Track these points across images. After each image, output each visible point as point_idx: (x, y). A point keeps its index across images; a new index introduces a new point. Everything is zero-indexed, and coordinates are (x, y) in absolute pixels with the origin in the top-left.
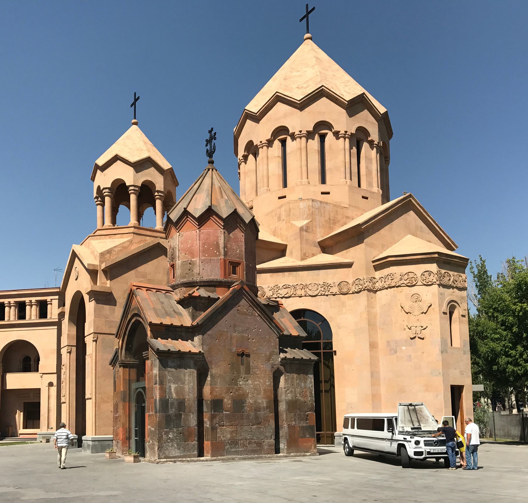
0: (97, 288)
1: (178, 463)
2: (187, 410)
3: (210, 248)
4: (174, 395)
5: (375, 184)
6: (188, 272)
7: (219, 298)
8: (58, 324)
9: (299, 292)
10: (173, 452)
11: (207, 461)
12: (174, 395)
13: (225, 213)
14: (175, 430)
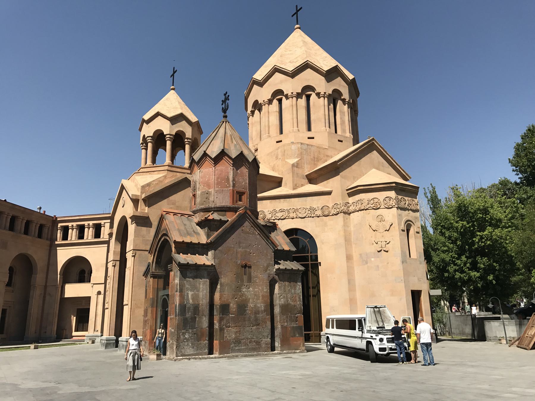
0: (137, 214)
1: (192, 360)
2: (201, 314)
3: (221, 182)
4: (191, 301)
6: (205, 199)
7: (228, 220)
8: (108, 243)
9: (292, 215)
11: (215, 358)
12: (191, 301)
13: (234, 154)
14: (190, 331)
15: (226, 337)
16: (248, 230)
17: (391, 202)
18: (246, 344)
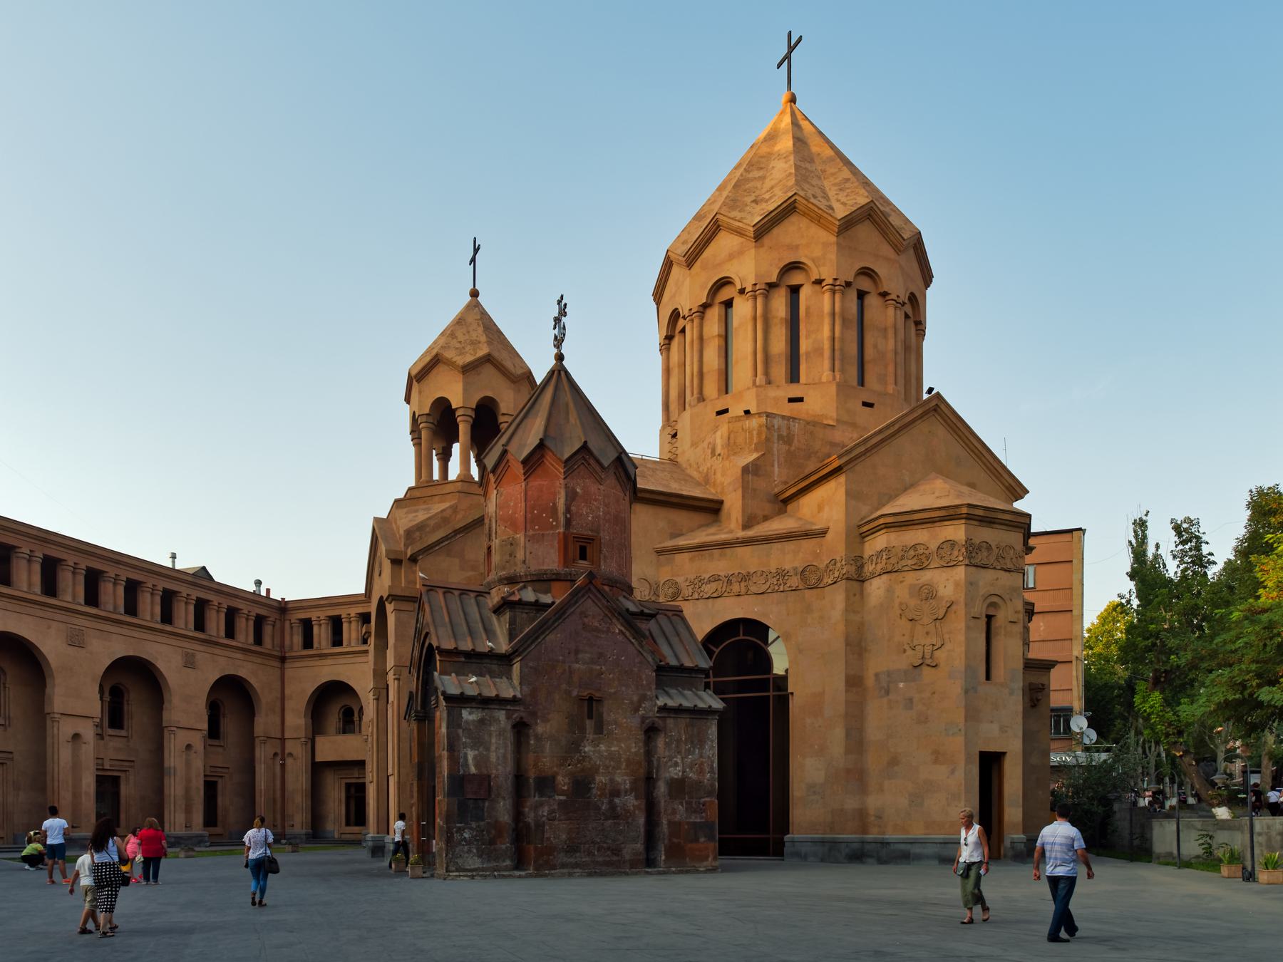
5: (891, 379)
12: (473, 770)
14: (474, 825)
15: (548, 839)
16: (596, 624)
18: (590, 853)
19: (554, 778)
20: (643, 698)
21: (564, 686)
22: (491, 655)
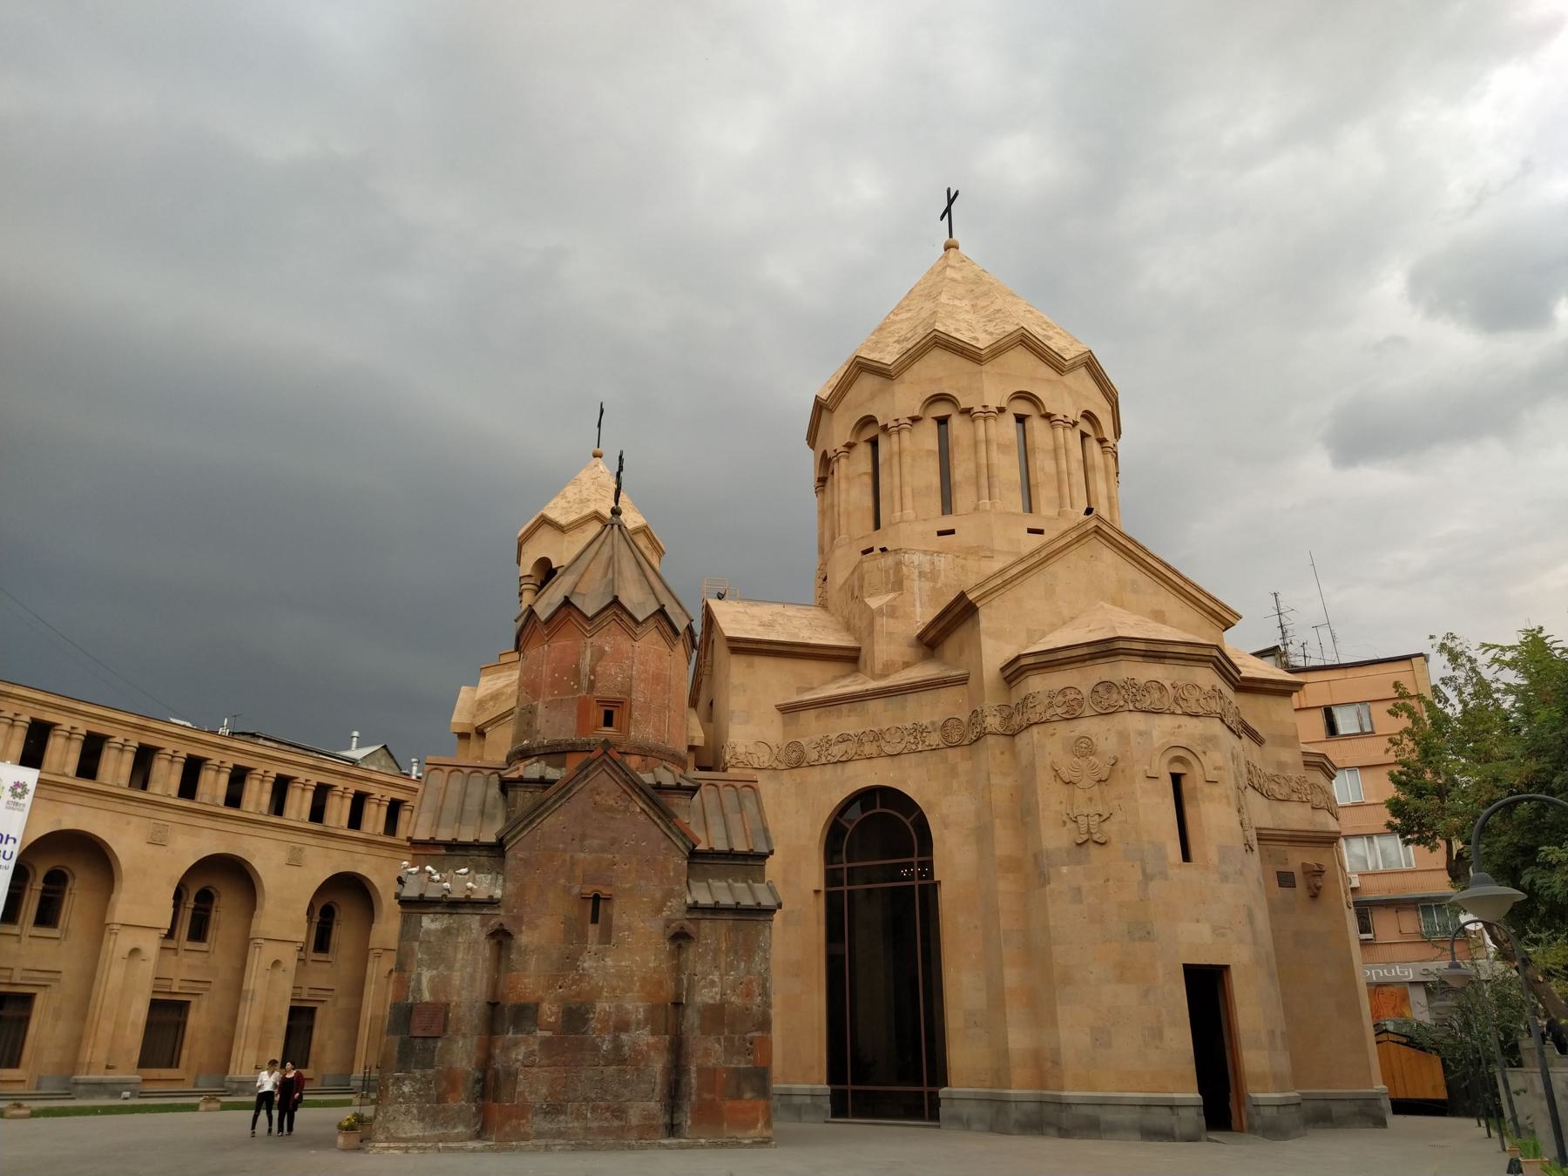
9: (869, 749)
10: (407, 1127)
14: (418, 1073)
15: (522, 1093)
16: (612, 802)
17: (1115, 696)
18: (579, 1116)
19: (537, 1005)
20: (669, 894)
21: (562, 881)
22: (476, 846)
